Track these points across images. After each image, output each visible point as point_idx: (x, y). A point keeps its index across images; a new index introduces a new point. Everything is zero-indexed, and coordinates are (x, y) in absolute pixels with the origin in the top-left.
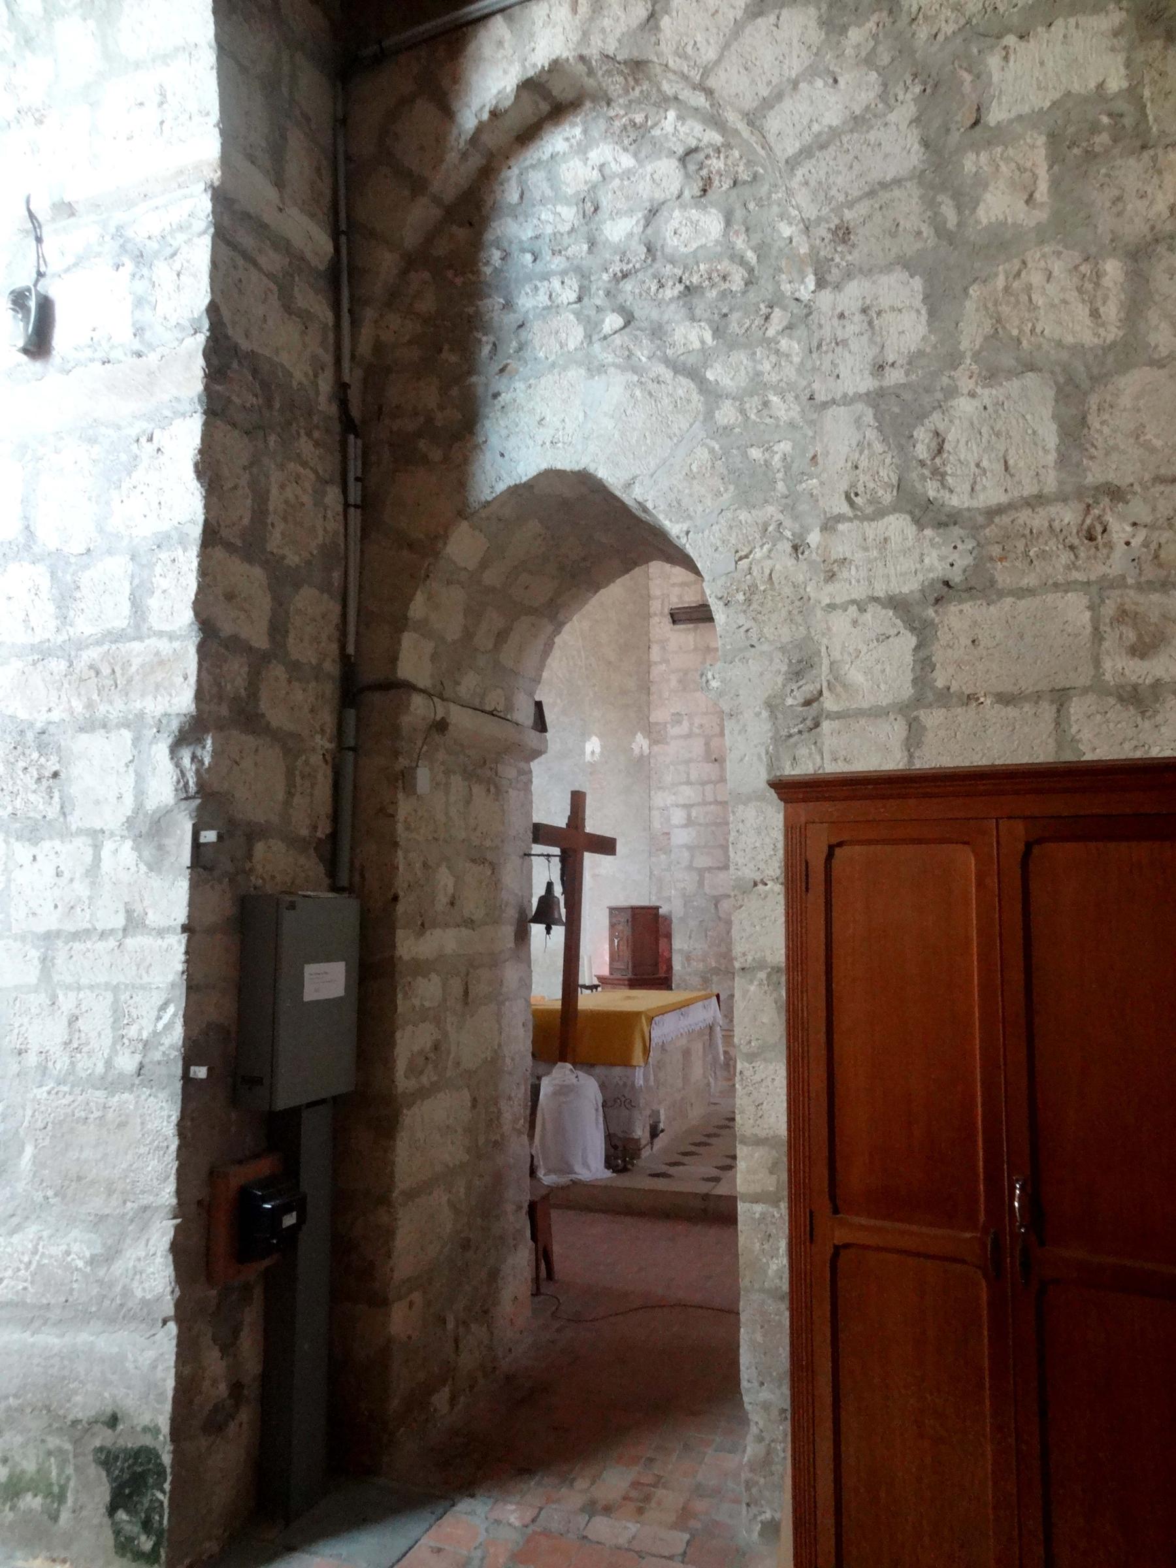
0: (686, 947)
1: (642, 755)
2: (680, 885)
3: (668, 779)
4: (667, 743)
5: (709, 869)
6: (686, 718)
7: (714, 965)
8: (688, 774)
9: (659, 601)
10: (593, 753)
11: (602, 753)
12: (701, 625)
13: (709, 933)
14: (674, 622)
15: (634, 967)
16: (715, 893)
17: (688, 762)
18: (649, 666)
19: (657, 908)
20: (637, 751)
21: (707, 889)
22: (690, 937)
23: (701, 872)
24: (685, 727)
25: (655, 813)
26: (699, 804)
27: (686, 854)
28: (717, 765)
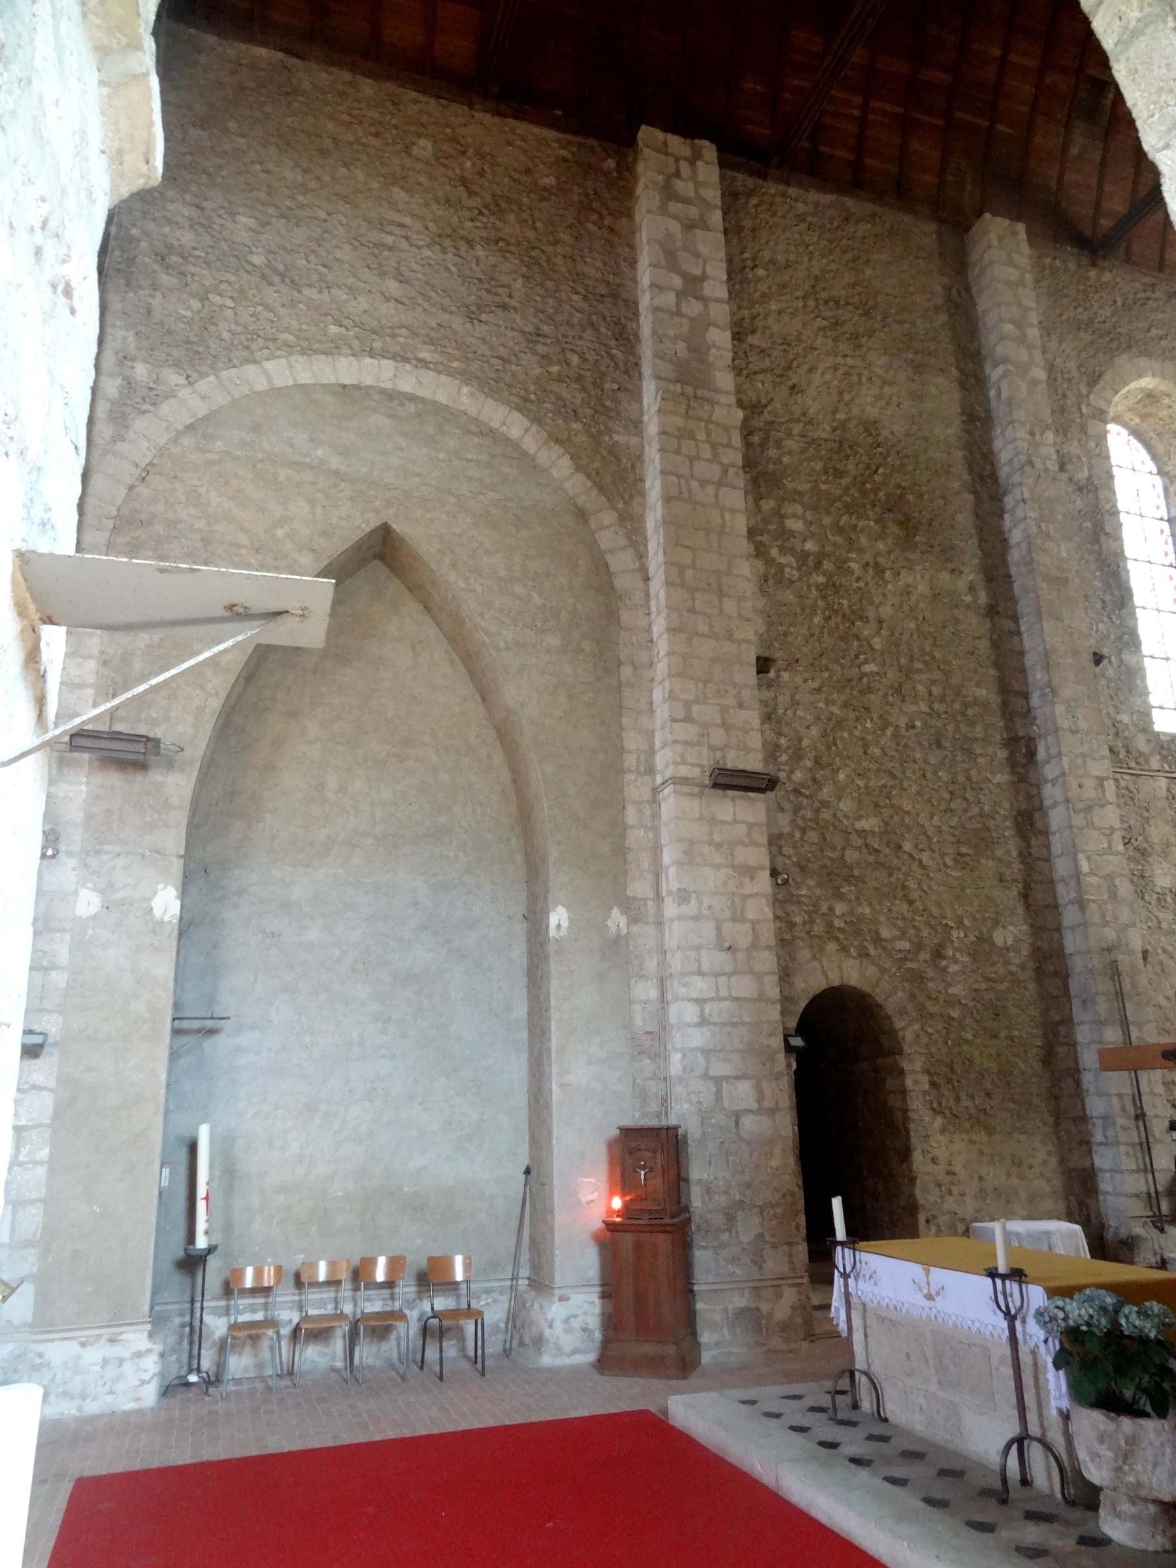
0: (705, 1177)
5: (727, 1078)
6: (693, 895)
7: (738, 1197)
8: (699, 962)
9: (635, 756)
10: (559, 926)
11: (570, 928)
16: (736, 1108)
17: (698, 948)
18: (625, 829)
20: (613, 929)
21: (726, 1103)
22: (710, 1163)
23: (718, 1081)
26: (713, 999)
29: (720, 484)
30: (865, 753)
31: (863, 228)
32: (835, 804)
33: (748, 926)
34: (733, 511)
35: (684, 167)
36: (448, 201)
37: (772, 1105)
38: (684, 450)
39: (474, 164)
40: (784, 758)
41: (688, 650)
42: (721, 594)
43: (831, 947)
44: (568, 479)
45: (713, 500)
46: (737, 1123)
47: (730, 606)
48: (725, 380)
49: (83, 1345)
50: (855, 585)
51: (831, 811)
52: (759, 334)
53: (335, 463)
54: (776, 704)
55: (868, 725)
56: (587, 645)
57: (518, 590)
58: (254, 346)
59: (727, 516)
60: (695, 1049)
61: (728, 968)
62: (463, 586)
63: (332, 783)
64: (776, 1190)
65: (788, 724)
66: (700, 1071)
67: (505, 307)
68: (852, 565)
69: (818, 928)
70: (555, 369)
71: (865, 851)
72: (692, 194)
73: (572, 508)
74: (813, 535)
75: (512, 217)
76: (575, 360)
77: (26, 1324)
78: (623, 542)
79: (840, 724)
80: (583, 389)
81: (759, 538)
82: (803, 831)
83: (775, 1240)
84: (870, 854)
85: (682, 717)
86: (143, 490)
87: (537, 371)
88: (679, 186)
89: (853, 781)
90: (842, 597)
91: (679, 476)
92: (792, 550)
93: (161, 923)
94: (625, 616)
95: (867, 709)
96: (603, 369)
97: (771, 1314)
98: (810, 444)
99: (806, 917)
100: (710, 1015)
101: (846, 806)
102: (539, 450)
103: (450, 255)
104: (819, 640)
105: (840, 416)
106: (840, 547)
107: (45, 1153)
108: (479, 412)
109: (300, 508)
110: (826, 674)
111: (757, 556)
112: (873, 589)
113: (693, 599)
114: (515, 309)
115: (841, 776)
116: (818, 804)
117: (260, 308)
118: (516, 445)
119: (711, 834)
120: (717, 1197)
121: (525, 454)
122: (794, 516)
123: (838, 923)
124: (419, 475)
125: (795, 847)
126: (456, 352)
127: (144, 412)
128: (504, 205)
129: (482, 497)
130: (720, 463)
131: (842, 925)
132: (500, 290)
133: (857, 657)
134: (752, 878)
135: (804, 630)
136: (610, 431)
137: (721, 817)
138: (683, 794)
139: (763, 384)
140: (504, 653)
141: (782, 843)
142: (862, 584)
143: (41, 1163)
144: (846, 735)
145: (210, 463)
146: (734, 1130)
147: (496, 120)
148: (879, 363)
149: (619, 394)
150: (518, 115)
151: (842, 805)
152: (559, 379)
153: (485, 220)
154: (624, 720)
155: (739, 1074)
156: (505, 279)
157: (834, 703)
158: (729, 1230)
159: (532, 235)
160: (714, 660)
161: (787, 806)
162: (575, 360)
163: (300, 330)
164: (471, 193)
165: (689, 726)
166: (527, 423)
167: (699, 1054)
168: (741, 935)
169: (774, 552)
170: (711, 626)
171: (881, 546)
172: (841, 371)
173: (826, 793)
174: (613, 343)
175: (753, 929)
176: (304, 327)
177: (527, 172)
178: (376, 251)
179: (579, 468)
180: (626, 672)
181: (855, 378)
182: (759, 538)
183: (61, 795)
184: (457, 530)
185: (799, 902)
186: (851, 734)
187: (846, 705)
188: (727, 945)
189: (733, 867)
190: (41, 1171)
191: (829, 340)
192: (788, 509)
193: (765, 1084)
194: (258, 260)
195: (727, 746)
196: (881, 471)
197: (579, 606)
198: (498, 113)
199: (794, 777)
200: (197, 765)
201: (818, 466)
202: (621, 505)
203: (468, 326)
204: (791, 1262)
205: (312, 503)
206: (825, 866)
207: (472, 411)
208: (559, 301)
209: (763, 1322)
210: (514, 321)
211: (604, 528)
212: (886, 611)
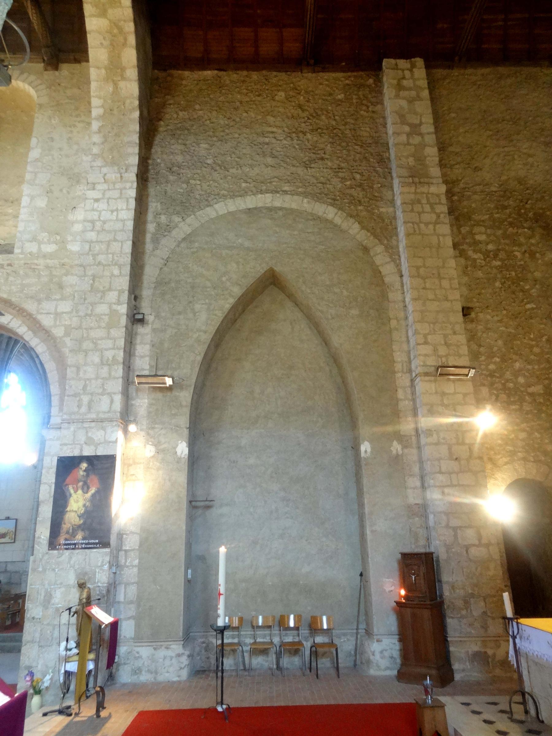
1: (398, 455)
7: (470, 591)
8: (440, 467)
9: (401, 364)
10: (366, 451)
11: (372, 452)
13: (465, 570)
20: (394, 452)
29: (436, 223)
31: (509, 81)
34: (444, 236)
35: (407, 74)
36: (293, 117)
38: (415, 209)
39: (304, 98)
41: (424, 308)
42: (440, 278)
44: (358, 233)
45: (432, 232)
47: (445, 284)
48: (435, 171)
49: (155, 649)
53: (247, 244)
57: (337, 290)
58: (210, 199)
59: (441, 238)
62: (309, 292)
63: (257, 389)
66: (444, 524)
67: (322, 159)
70: (348, 183)
72: (412, 85)
73: (360, 247)
75: (323, 117)
76: (358, 177)
77: (131, 638)
78: (388, 259)
80: (363, 190)
83: (494, 615)
86: (166, 269)
87: (340, 185)
88: (405, 83)
91: (413, 223)
92: (480, 251)
93: (180, 458)
97: (494, 655)
102: (342, 222)
103: (295, 141)
105: (504, 178)
107: (136, 562)
108: (313, 210)
109: (233, 266)
111: (461, 256)
113: (425, 283)
114: (327, 159)
117: (211, 182)
118: (331, 222)
119: (442, 400)
120: (458, 591)
121: (336, 226)
122: (480, 233)
124: (286, 243)
126: (300, 184)
127: (165, 236)
128: (320, 113)
129: (316, 249)
130: (435, 213)
132: (319, 152)
135: (490, 291)
136: (378, 207)
138: (426, 381)
143: (136, 566)
145: (193, 253)
147: (314, 75)
148: (524, 146)
149: (381, 189)
150: (324, 70)
152: (351, 187)
153: (310, 121)
154: (394, 347)
156: (322, 146)
158: (467, 609)
159: (334, 123)
160: (438, 312)
162: (358, 177)
163: (229, 188)
164: (303, 111)
165: (426, 347)
166: (336, 210)
169: (470, 253)
170: (435, 295)
171: (533, 241)
173: (508, 375)
174: (377, 165)
176: (231, 186)
177: (330, 95)
178: (261, 146)
179: (363, 228)
180: (394, 323)
182: (461, 247)
183: (138, 404)
184: (304, 266)
188: (455, 457)
190: (135, 570)
192: (476, 229)
194: (209, 162)
196: (529, 202)
198: (314, 72)
200: (193, 387)
201: (492, 206)
202: (386, 242)
205: (238, 263)
207: (310, 211)
208: (349, 151)
209: (490, 660)
210: (326, 164)
211: (378, 254)
212: (538, 275)
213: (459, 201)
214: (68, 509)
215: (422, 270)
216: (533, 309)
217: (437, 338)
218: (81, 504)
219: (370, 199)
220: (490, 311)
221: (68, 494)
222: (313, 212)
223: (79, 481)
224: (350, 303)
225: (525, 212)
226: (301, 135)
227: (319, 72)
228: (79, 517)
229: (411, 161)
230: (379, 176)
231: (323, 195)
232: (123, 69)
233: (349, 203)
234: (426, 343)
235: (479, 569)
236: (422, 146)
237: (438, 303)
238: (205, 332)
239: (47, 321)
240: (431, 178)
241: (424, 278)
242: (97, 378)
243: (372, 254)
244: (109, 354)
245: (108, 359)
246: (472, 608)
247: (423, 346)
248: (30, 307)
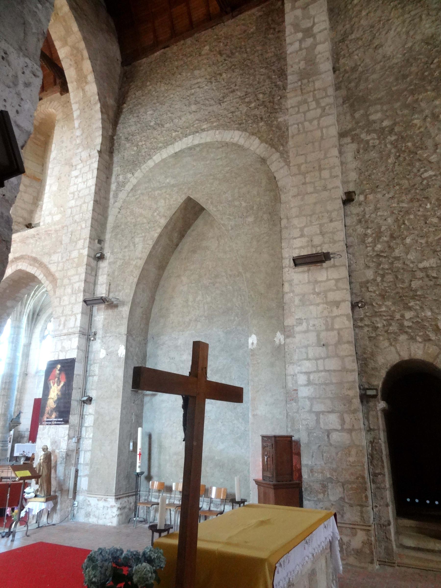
0: (310, 463)
1: (280, 344)
2: (304, 423)
3: (296, 357)
4: (294, 337)
5: (323, 412)
6: (304, 321)
7: (328, 476)
8: (307, 354)
9: (288, 260)
10: (253, 344)
11: (257, 344)
12: (312, 267)
13: (325, 454)
14: (296, 265)
15: (277, 475)
16: (327, 428)
17: (307, 347)
18: (283, 295)
19: (291, 437)
20: (277, 342)
22: (313, 457)
23: (318, 414)
24: (304, 326)
25: (289, 378)
26: (315, 372)
27: (308, 403)
28: (324, 348)
29: (321, 116)
30: (426, 223)
32: (405, 257)
33: (335, 332)
37: (351, 427)
40: (370, 240)
41: (302, 203)
42: (320, 169)
43: (403, 337)
44: (258, 148)
46: (328, 436)
47: (326, 174)
49: (98, 500)
50: (418, 132)
51: (401, 262)
52: (355, 31)
53: (173, 182)
54: (365, 213)
55: (428, 206)
56: (265, 217)
57: (237, 203)
58: (151, 153)
60: (305, 397)
61: (323, 355)
62: (215, 210)
63: (191, 298)
64: (352, 474)
65: (372, 222)
66: (307, 408)
68: (415, 121)
69: (394, 328)
70: (253, 105)
71: (426, 279)
74: (388, 116)
75: (237, 54)
77: (86, 490)
78: (283, 164)
79: (407, 212)
81: (353, 133)
82: (383, 276)
83: (352, 502)
84: (431, 280)
85: (299, 235)
86: (119, 216)
87: (246, 109)
89: (417, 241)
90: (408, 142)
92: (375, 131)
93: (120, 358)
94: (283, 197)
95: (427, 198)
96: (273, 93)
97: (349, 543)
98: (386, 71)
99: (385, 323)
100: (313, 380)
101: (412, 256)
102: (245, 142)
104: (393, 171)
105: (409, 45)
106: (406, 116)
107: (91, 436)
109: (162, 203)
110: (397, 187)
112: (431, 130)
113: (305, 178)
114: (237, 90)
115: (408, 241)
116: (392, 259)
117: (152, 140)
119: (314, 289)
120: (316, 474)
121: (240, 146)
122: (377, 112)
123: (406, 323)
124: (200, 173)
125: (378, 285)
126: (215, 119)
127: (121, 191)
128: (234, 51)
130: (321, 107)
131: (411, 324)
133: (419, 171)
134: (338, 307)
135: (383, 168)
136: (276, 118)
137: (319, 279)
138: (299, 272)
139: (358, 55)
140: (231, 231)
141: (369, 285)
142: (422, 129)
143: (90, 438)
144: (412, 217)
145: (136, 199)
146: (327, 440)
147: (233, 20)
151: (409, 257)
155: (330, 410)
156: (234, 80)
157: (402, 202)
158: (324, 493)
159: (245, 56)
160: (315, 204)
161: (372, 265)
162: (261, 96)
163: (164, 140)
166: (240, 133)
167: (307, 400)
168: (332, 337)
169: (363, 136)
170: (315, 187)
172: (408, 21)
173: (397, 253)
175: (339, 334)
176: (165, 138)
178: (188, 98)
179: (262, 142)
180: (284, 222)
181: (417, 20)
182: (353, 133)
183: (97, 320)
184: (213, 189)
185: (381, 315)
186: (415, 215)
187: (411, 200)
188: (322, 343)
189: (327, 303)
190: (91, 441)
191: (400, 11)
192: (372, 110)
193: (346, 416)
194: (152, 124)
195: (324, 243)
197: (262, 201)
198: (233, 17)
199: (376, 249)
200: (130, 303)
201: (391, 79)
203: (219, 106)
204: (362, 517)
205: (165, 199)
206: (398, 293)
207: (219, 140)
209: (344, 547)
211: (273, 162)
213: (356, 86)
214: (49, 397)
215: (303, 168)
216: (431, 177)
217: (315, 229)
218: (56, 392)
219: (271, 113)
220: (379, 190)
221: (50, 387)
222: (223, 140)
223: (55, 378)
224: (248, 211)
225: (429, 74)
226: (218, 77)
227: (237, 16)
228: (54, 402)
229: (302, 65)
230: (279, 88)
231: (232, 123)
232: (86, 77)
233: (252, 123)
234: (302, 236)
235: (340, 454)
236: (314, 46)
237: (316, 195)
238: (140, 259)
239: (53, 268)
240: (320, 74)
241: (304, 174)
242: (69, 304)
243: (268, 164)
244: (76, 286)
245: (76, 289)
246: (329, 493)
247: (299, 239)
248: (45, 260)
